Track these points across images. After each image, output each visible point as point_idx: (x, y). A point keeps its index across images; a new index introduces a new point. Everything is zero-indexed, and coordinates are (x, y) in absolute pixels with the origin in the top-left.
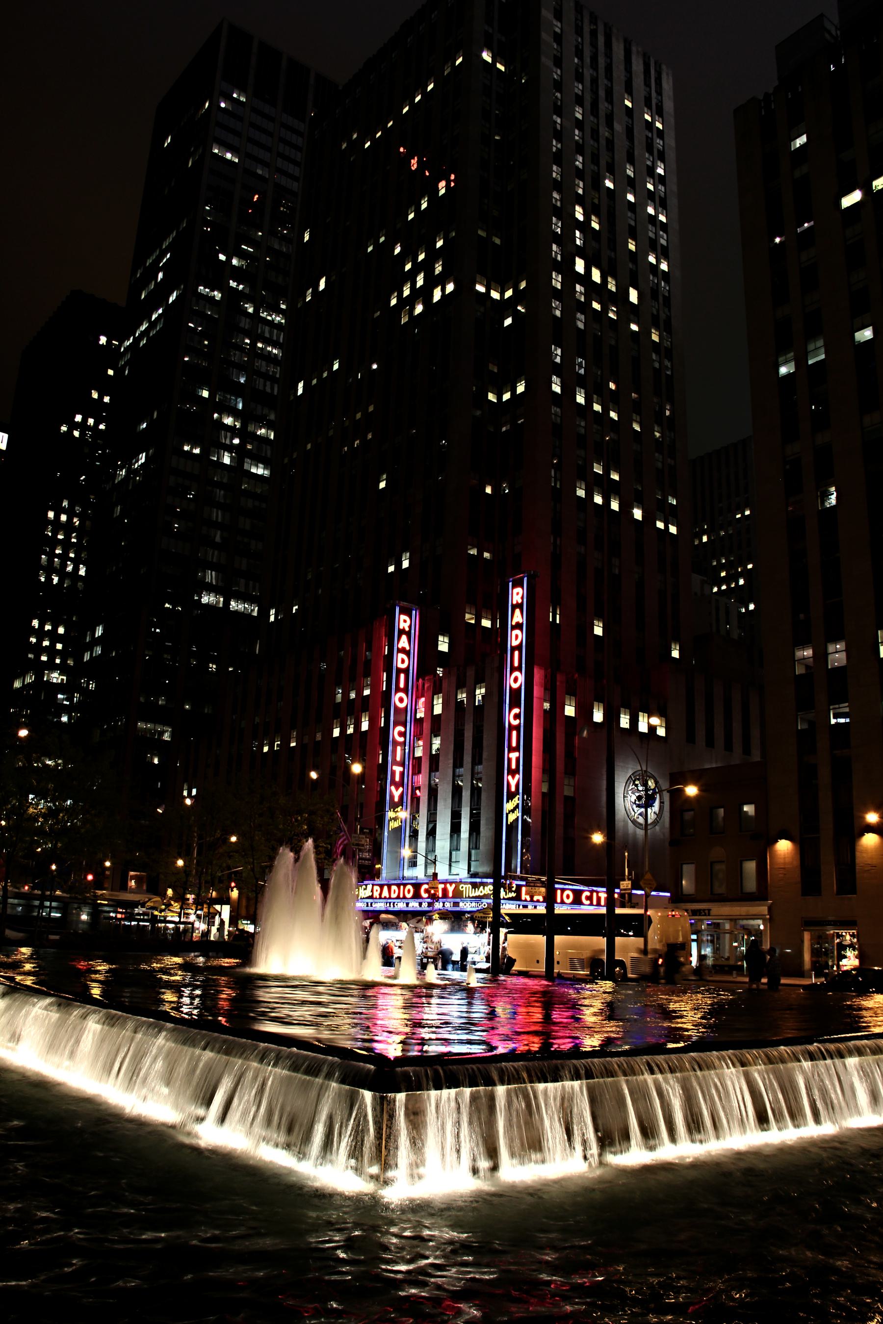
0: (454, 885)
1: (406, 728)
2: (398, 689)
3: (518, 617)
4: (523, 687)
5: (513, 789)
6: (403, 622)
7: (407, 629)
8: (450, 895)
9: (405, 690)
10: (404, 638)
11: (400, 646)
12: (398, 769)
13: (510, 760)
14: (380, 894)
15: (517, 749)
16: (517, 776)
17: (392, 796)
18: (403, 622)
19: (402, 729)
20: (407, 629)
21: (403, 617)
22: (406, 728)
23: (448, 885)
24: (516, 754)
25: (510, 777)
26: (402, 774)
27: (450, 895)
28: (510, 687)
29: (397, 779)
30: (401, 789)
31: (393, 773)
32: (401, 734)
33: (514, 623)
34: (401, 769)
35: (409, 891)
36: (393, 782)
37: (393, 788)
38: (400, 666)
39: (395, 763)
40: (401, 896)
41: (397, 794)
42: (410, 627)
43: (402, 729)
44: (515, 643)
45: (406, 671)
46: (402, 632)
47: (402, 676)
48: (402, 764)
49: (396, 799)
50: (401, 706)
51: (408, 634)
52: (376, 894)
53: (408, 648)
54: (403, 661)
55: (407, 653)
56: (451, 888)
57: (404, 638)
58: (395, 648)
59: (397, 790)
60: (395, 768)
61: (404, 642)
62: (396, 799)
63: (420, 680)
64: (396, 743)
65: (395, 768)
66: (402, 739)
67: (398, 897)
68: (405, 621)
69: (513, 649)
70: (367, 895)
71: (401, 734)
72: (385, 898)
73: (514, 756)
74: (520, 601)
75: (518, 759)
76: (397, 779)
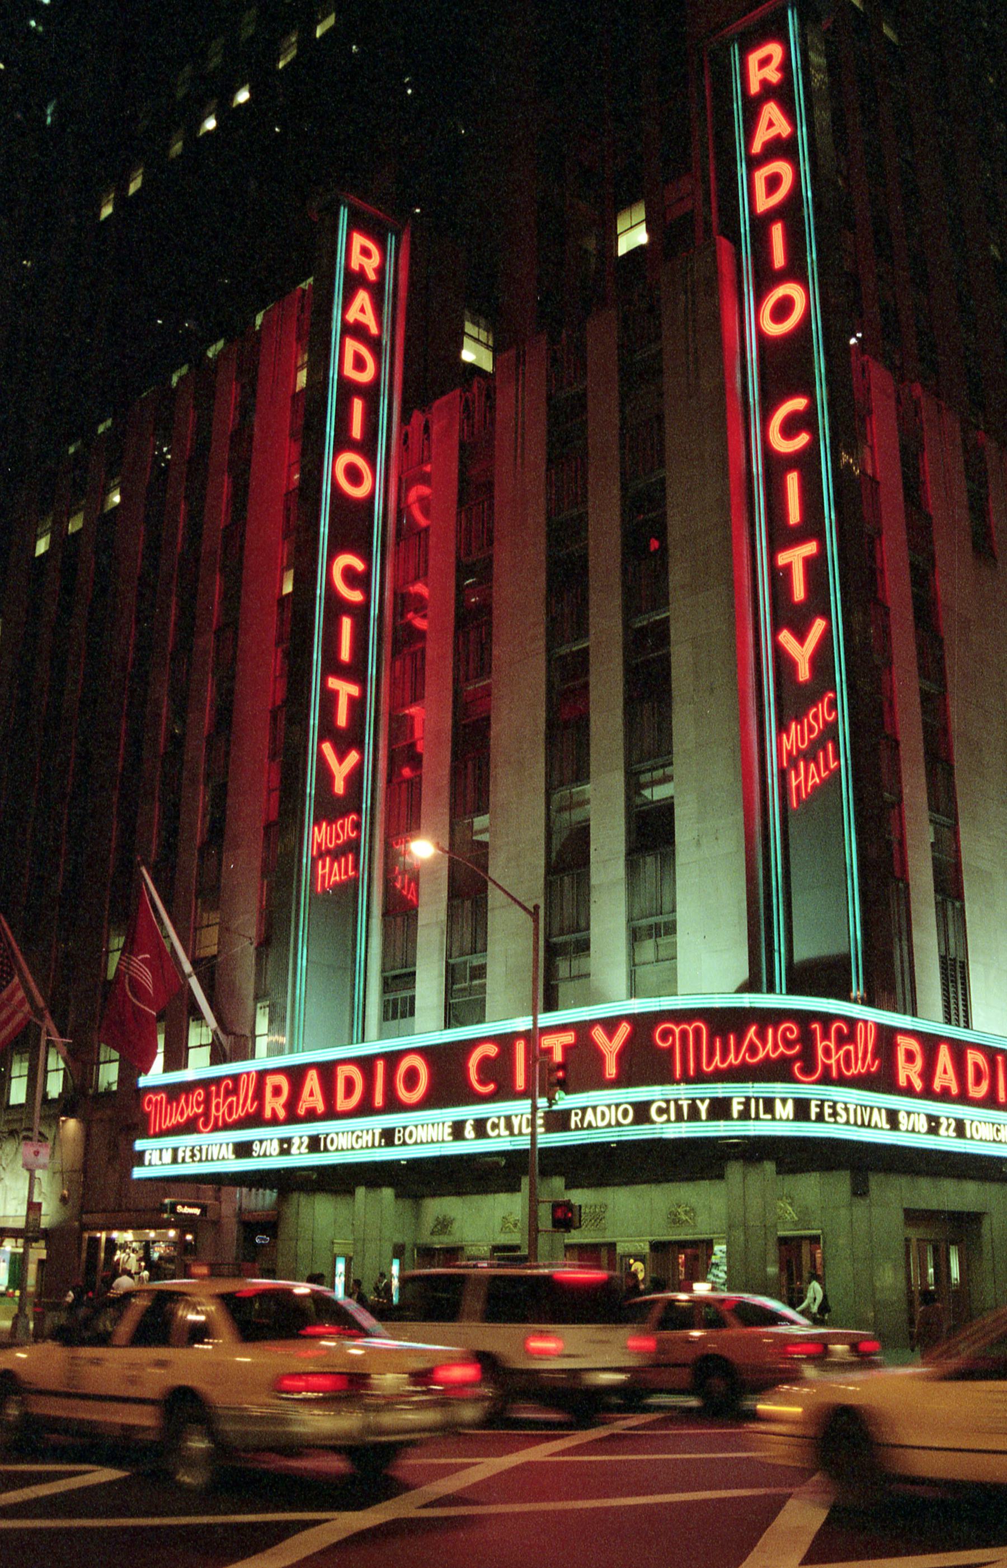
1: (367, 559)
2: (344, 442)
4: (817, 326)
6: (359, 253)
7: (372, 276)
9: (367, 448)
10: (362, 298)
11: (352, 315)
12: (345, 689)
13: (780, 578)
14: (291, 1105)
15: (811, 528)
16: (819, 626)
17: (325, 775)
18: (359, 253)
19: (359, 565)
20: (372, 276)
21: (359, 240)
22: (367, 559)
24: (810, 548)
25: (786, 637)
26: (357, 705)
28: (760, 333)
29: (342, 719)
30: (353, 757)
31: (330, 698)
32: (355, 579)
33: (757, 148)
34: (354, 690)
36: (328, 730)
37: (327, 748)
38: (349, 371)
39: (333, 666)
40: (379, 1100)
41: (340, 771)
42: (380, 271)
43: (359, 565)
44: (764, 203)
45: (370, 393)
46: (355, 281)
47: (358, 406)
48: (355, 672)
49: (339, 787)
50: (359, 492)
51: (376, 292)
52: (275, 1105)
53: (374, 330)
54: (360, 364)
55: (374, 344)
56: (610, 1047)
57: (362, 298)
58: (336, 326)
59: (341, 760)
60: (333, 683)
61: (361, 309)
62: (339, 787)
63: (418, 418)
64: (336, 606)
65: (333, 683)
66: (355, 596)
68: (365, 252)
69: (761, 225)
70: (239, 1113)
71: (350, 576)
73: (795, 557)
75: (815, 567)
76: (342, 719)
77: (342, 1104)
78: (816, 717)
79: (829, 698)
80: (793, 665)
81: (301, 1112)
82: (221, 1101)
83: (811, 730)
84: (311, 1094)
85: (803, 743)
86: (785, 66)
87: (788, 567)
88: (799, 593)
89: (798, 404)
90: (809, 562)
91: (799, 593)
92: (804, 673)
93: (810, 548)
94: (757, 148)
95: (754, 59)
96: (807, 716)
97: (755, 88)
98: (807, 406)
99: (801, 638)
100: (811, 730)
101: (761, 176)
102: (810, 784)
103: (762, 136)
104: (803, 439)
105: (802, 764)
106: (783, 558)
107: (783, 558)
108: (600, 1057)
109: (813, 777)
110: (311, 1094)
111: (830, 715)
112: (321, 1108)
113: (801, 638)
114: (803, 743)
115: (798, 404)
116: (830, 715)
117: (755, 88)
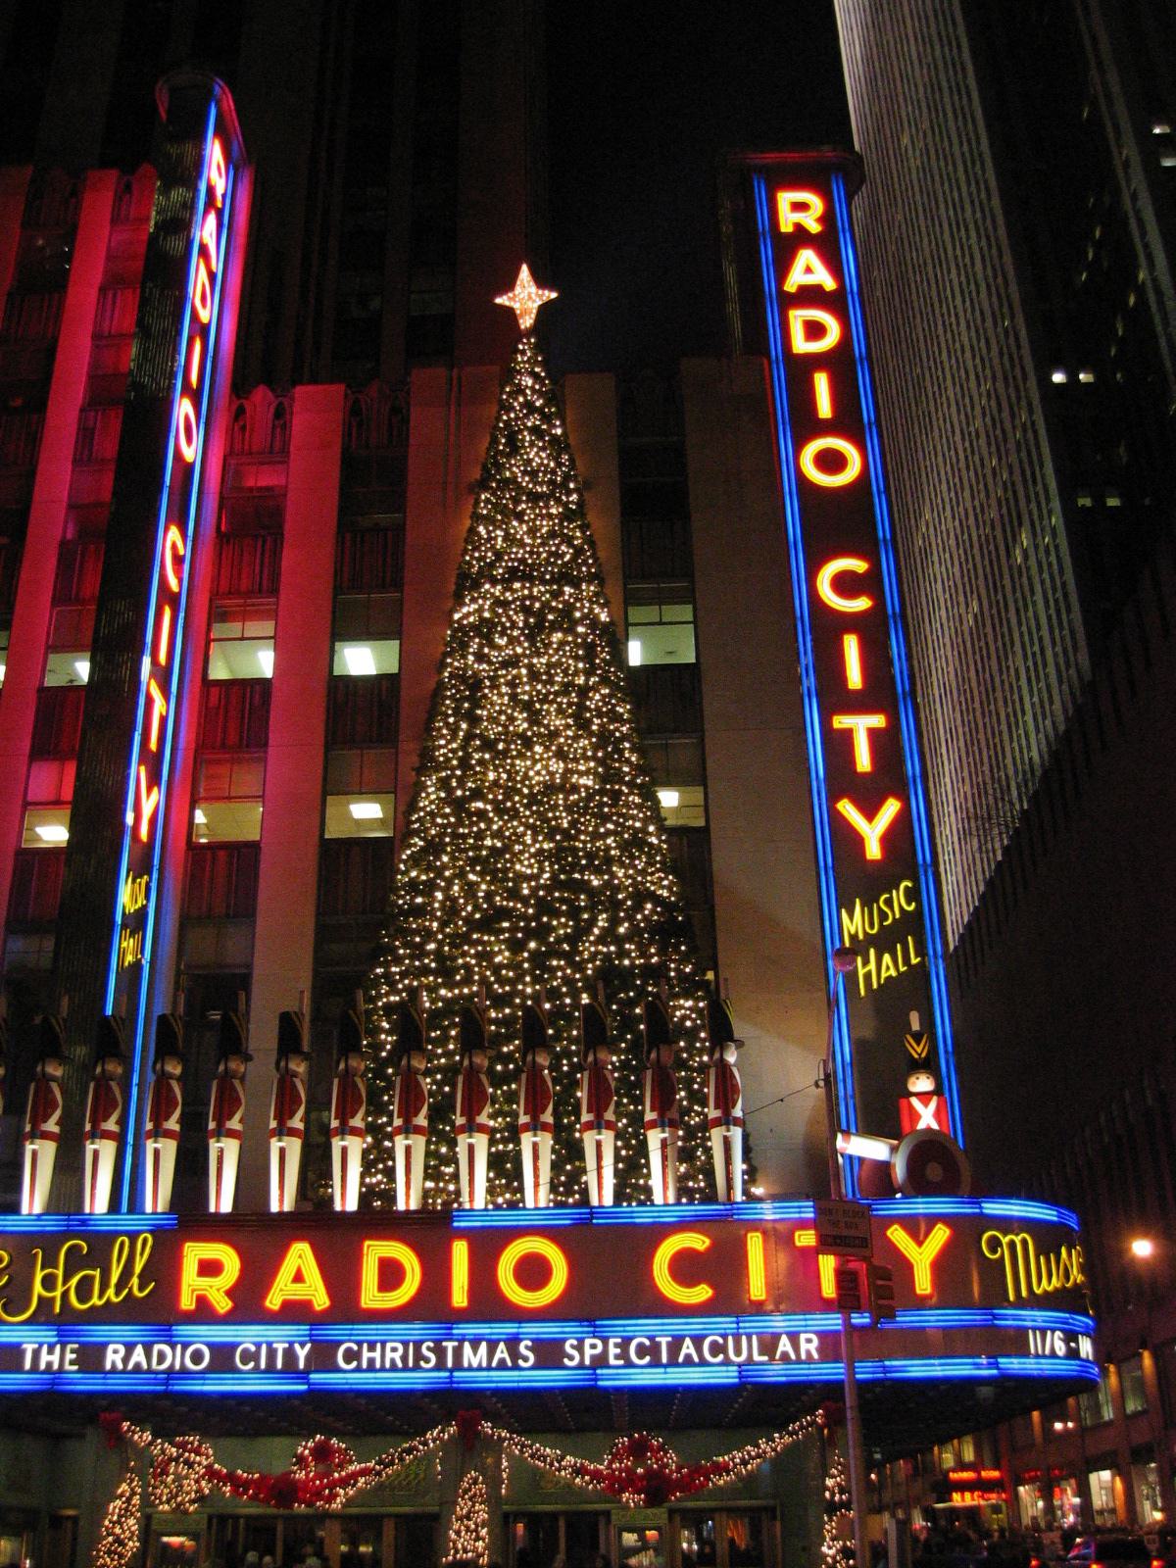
0: (940, 1235)
3: (808, 269)
5: (873, 851)
8: (923, 1283)
13: (839, 745)
16: (891, 808)
23: (898, 1235)
24: (878, 721)
25: (847, 808)
27: (923, 1283)
33: (791, 286)
35: (533, 1272)
44: (801, 345)
67: (431, 1305)
72: (295, 1312)
74: (814, 228)
77: (370, 1296)
78: (889, 903)
79: (907, 887)
80: (858, 841)
81: (273, 1302)
82: (60, 1273)
83: (883, 916)
84: (298, 1278)
85: (872, 926)
86: (827, 219)
87: (847, 735)
88: (863, 761)
89: (859, 566)
90: (873, 733)
91: (863, 761)
92: (873, 851)
93: (878, 721)
94: (791, 286)
95: (785, 199)
96: (878, 903)
97: (786, 227)
98: (867, 573)
99: (870, 814)
100: (883, 916)
101: (797, 317)
102: (884, 975)
103: (796, 279)
104: (862, 604)
105: (872, 952)
106: (840, 722)
107: (840, 722)
108: (907, 1267)
109: (888, 968)
110: (298, 1278)
111: (909, 904)
112: (321, 1300)
113: (870, 814)
114: (872, 926)
115: (859, 566)
116: (909, 904)
117: (786, 227)
